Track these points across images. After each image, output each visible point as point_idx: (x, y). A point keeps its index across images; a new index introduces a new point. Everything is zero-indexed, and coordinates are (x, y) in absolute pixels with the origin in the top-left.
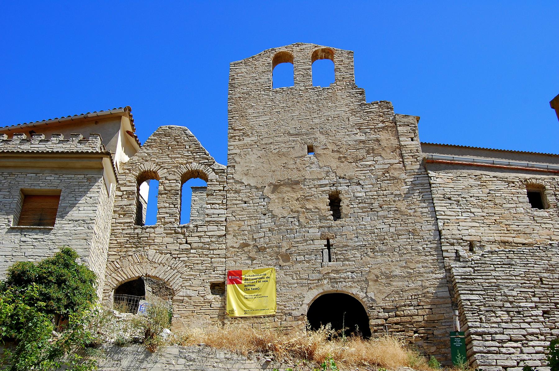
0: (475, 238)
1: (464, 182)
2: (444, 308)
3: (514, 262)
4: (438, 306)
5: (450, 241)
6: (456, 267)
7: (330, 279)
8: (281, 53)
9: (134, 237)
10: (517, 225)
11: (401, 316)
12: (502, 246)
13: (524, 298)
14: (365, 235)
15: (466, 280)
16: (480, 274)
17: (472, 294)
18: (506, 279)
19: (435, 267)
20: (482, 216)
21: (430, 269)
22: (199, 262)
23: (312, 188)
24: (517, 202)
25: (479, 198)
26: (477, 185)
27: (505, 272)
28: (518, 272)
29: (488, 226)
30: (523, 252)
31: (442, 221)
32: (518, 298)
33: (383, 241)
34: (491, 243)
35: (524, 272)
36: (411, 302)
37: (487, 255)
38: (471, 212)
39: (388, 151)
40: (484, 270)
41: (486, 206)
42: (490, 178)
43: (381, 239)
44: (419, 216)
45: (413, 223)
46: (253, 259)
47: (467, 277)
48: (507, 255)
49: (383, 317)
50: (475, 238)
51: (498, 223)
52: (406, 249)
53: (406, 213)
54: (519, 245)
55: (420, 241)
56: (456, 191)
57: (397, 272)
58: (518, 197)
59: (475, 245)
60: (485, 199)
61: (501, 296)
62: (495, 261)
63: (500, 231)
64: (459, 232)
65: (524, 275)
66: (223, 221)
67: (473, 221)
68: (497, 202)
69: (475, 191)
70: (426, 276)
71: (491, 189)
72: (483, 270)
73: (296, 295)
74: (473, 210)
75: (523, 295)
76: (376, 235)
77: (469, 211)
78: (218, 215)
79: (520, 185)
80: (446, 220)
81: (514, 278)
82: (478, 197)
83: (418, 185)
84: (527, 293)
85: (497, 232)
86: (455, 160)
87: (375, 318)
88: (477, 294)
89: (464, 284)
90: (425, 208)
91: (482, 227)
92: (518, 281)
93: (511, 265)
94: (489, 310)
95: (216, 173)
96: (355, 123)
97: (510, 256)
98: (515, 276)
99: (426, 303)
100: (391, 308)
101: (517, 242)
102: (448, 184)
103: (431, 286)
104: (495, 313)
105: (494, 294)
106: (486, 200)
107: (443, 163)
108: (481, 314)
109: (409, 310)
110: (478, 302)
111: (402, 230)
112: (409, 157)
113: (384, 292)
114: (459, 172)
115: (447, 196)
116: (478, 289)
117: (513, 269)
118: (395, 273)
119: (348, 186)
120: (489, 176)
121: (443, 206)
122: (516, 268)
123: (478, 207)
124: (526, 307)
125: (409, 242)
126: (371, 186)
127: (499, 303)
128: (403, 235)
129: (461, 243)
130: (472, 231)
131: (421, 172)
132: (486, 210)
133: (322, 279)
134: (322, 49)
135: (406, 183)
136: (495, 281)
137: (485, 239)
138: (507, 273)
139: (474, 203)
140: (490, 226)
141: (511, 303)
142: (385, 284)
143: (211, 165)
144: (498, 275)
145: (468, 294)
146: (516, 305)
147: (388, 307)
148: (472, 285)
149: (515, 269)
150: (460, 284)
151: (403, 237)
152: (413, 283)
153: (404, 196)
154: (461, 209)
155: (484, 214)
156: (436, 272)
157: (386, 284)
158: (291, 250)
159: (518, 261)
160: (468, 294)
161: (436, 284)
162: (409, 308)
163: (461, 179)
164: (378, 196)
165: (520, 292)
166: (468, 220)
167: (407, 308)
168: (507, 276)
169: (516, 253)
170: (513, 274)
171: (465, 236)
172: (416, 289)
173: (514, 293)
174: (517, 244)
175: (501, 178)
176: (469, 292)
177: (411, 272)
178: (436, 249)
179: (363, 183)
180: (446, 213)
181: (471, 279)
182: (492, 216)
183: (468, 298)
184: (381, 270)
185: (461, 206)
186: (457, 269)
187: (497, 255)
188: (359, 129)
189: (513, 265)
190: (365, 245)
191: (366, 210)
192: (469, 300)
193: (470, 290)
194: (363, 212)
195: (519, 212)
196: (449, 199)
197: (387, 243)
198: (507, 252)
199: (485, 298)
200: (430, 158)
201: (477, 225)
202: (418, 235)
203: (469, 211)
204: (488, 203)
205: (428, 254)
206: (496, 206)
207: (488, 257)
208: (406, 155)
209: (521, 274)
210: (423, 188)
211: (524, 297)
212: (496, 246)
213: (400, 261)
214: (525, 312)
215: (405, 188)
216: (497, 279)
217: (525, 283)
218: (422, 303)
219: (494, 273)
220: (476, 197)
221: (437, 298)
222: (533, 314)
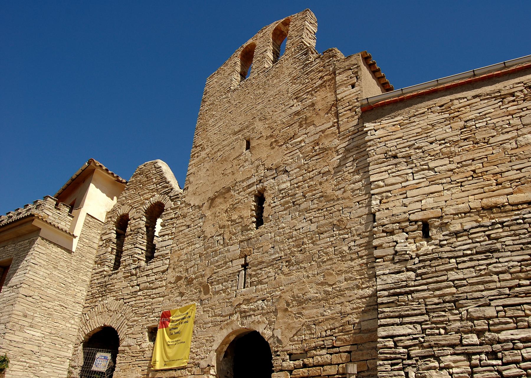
0: (432, 213)
1: (421, 122)
2: (368, 349)
3: (499, 246)
4: (360, 347)
5: (387, 228)
6: (384, 274)
7: (241, 312)
8: (249, 47)
9: (103, 285)
10: (517, 170)
11: (310, 365)
12: (485, 216)
13: (511, 320)
14: (282, 242)
15: (397, 297)
16: (424, 281)
17: (402, 324)
18: (478, 283)
19: (363, 277)
20: (448, 171)
21: (355, 282)
22: (142, 304)
23: (241, 191)
24: (519, 127)
25: (446, 141)
26: (443, 120)
27: (478, 268)
28: (506, 264)
29: (459, 184)
30: (523, 219)
31: (379, 197)
32: (496, 320)
33: (300, 245)
34: (463, 215)
35: (518, 262)
36: (323, 341)
37: (446, 240)
38: (429, 169)
39: (322, 113)
40: (436, 271)
41: (457, 150)
42: (468, 100)
43: (299, 245)
44: (348, 198)
45: (340, 211)
46: (182, 294)
47: (398, 290)
48: (487, 233)
49: (287, 369)
50: (432, 213)
51: (480, 175)
52: (326, 253)
53: (332, 198)
54: (520, 207)
55: (346, 236)
56: (406, 140)
57: (312, 293)
58: (520, 117)
59: (433, 226)
60: (455, 139)
61: (461, 320)
62: (460, 250)
63: (483, 188)
64: (405, 209)
65: (519, 269)
66: (168, 254)
67: (433, 182)
68: (479, 137)
69: (439, 133)
70: (348, 295)
71: (468, 118)
72: (432, 272)
73: (207, 338)
74: (432, 165)
75: (509, 314)
76: (294, 239)
77: (426, 167)
78: (165, 247)
79: (525, 95)
80: (384, 194)
81: (495, 277)
82: (444, 140)
83: (352, 150)
84: (519, 307)
85: (476, 191)
86: (404, 94)
87: (278, 370)
88: (411, 323)
89: (393, 305)
90: (358, 182)
91: (448, 190)
92: (503, 284)
93: (491, 252)
94: (427, 354)
95: (172, 200)
96: (293, 93)
97: (493, 233)
98: (497, 273)
99: (344, 343)
100: (298, 352)
101: (516, 201)
102: (394, 133)
103: (353, 311)
104: (439, 362)
105: (446, 318)
106: (458, 141)
107: (388, 105)
108: (409, 365)
109: (320, 355)
110: (408, 340)
111: (325, 225)
112: (345, 112)
113: (293, 328)
114: (412, 110)
115: (390, 153)
116: (416, 312)
117: (495, 260)
118: (309, 296)
119: (274, 178)
120: (466, 98)
121: (382, 172)
122: (502, 257)
123: (442, 157)
124: (512, 340)
125: (332, 241)
126: (298, 169)
127: (452, 337)
128: (326, 232)
129: (407, 227)
130: (428, 202)
131: (358, 129)
132: (457, 159)
133: (233, 314)
134: (282, 23)
135: (337, 151)
136: (454, 290)
137: (450, 210)
138: (480, 270)
139: (435, 152)
140: (463, 184)
141: (480, 333)
142: (295, 314)
143: (169, 193)
144: (461, 276)
145: (393, 324)
146: (490, 337)
147: (294, 352)
148: (407, 304)
149: (501, 260)
150: (385, 306)
151: (326, 235)
152: (330, 308)
153: (333, 172)
154: (412, 168)
155: (453, 166)
156: (364, 286)
157: (297, 313)
158: (212, 278)
159: (508, 241)
160: (393, 324)
161: (360, 308)
162: (321, 352)
163: (415, 120)
164: (304, 181)
165: (504, 306)
166: (423, 185)
167: (318, 353)
168: (481, 275)
169: (507, 226)
170: (494, 270)
171: (414, 213)
172: (333, 319)
173: (490, 312)
174: (517, 205)
175: (488, 94)
176: (397, 320)
177: (328, 291)
178: (366, 246)
179: (289, 169)
180: (387, 182)
181: (407, 293)
182: (467, 166)
183: (391, 333)
184: (293, 292)
185: (412, 163)
186: (385, 277)
187: (466, 238)
188: (297, 98)
189: (497, 250)
190: (281, 257)
191: (287, 205)
192: (392, 337)
193: (400, 317)
194: (285, 210)
195: (522, 143)
196: (395, 157)
197: (305, 248)
198: (488, 226)
199: (426, 329)
200: (365, 105)
201: (440, 188)
202: (345, 228)
203: (426, 167)
204: (462, 144)
205: (354, 256)
206: (476, 146)
207: (448, 244)
208: (343, 110)
209: (513, 266)
210: (358, 151)
211: (510, 317)
212: (473, 219)
213: (318, 275)
214: (506, 353)
215: (336, 159)
216: (457, 287)
217: (519, 286)
218: (338, 343)
219: (453, 275)
220: (439, 141)
221: (360, 331)
222: (525, 355)
